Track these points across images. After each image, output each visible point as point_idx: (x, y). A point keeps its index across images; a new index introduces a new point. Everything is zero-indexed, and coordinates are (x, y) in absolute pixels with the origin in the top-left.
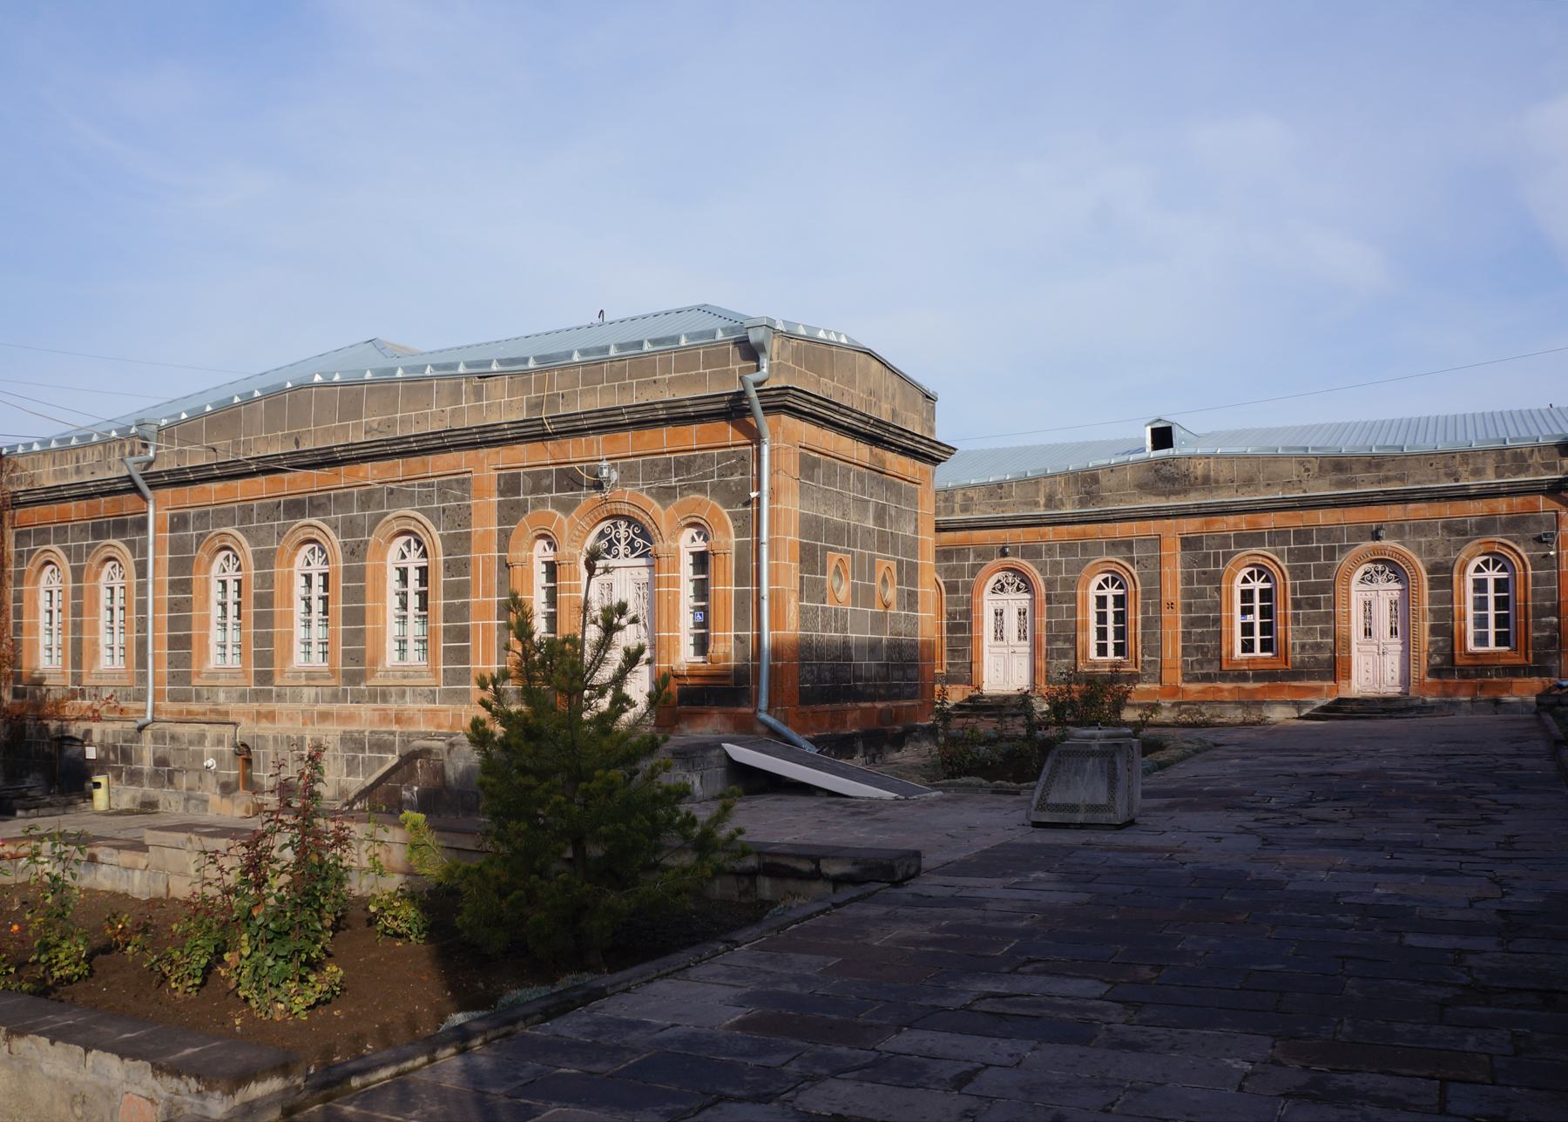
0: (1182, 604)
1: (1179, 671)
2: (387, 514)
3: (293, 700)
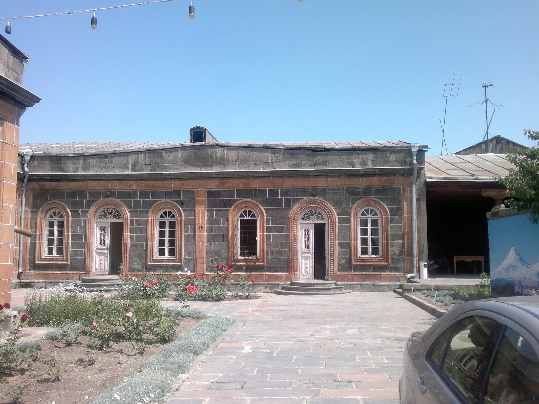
0: (207, 227)
1: (205, 264)
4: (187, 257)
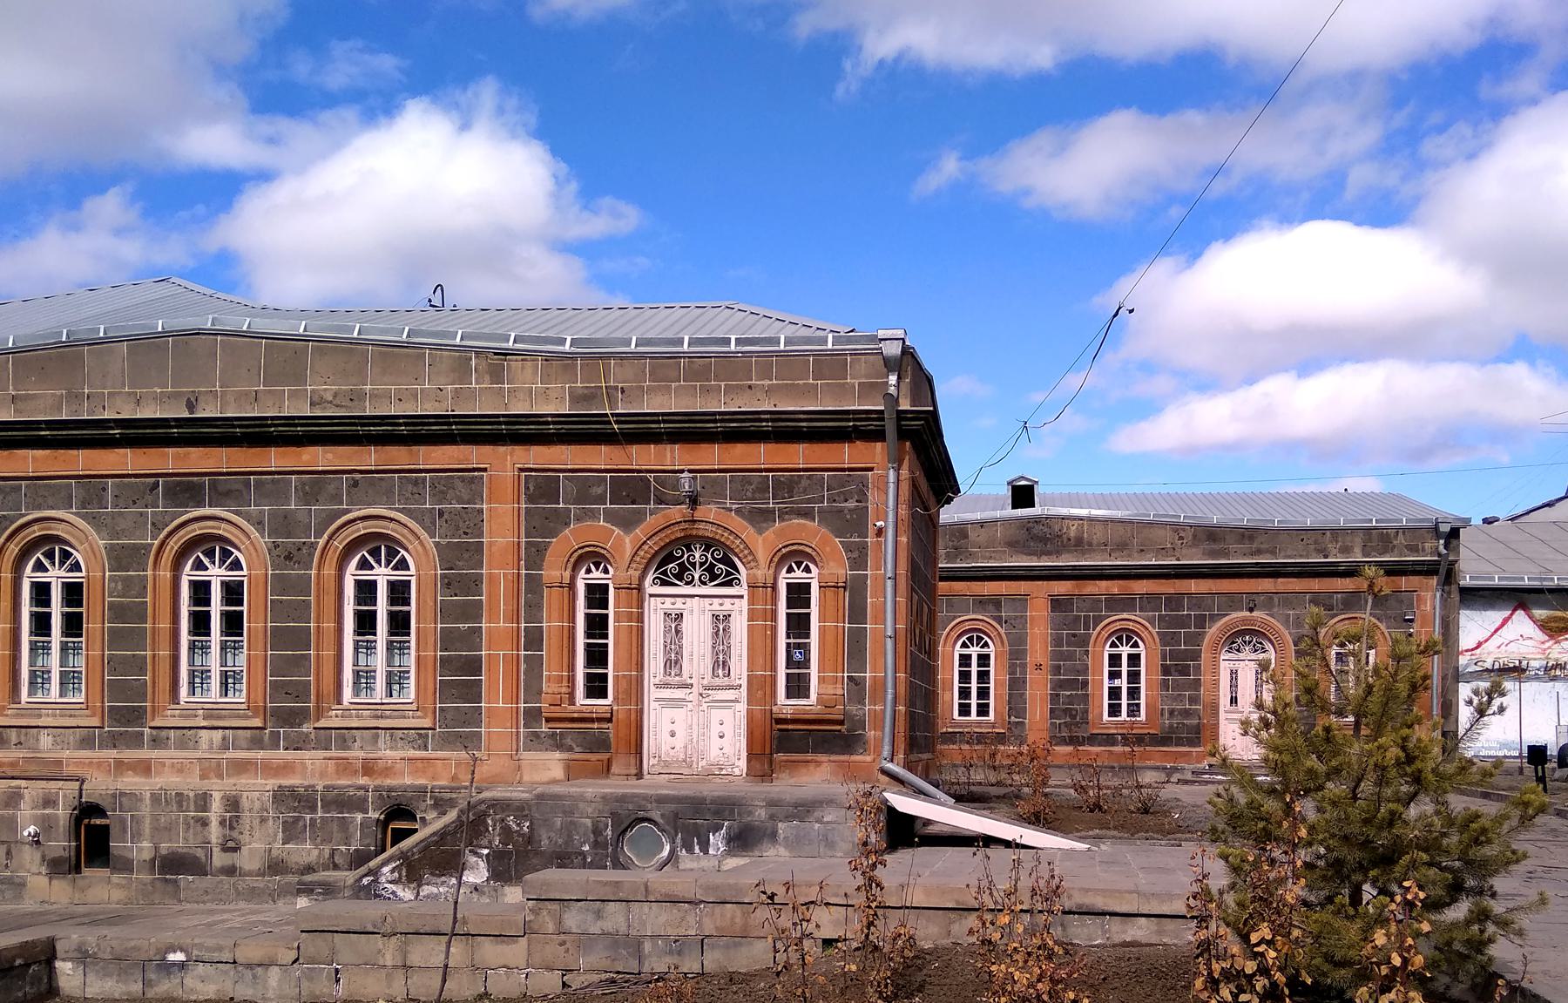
2: (348, 511)
3: (182, 745)
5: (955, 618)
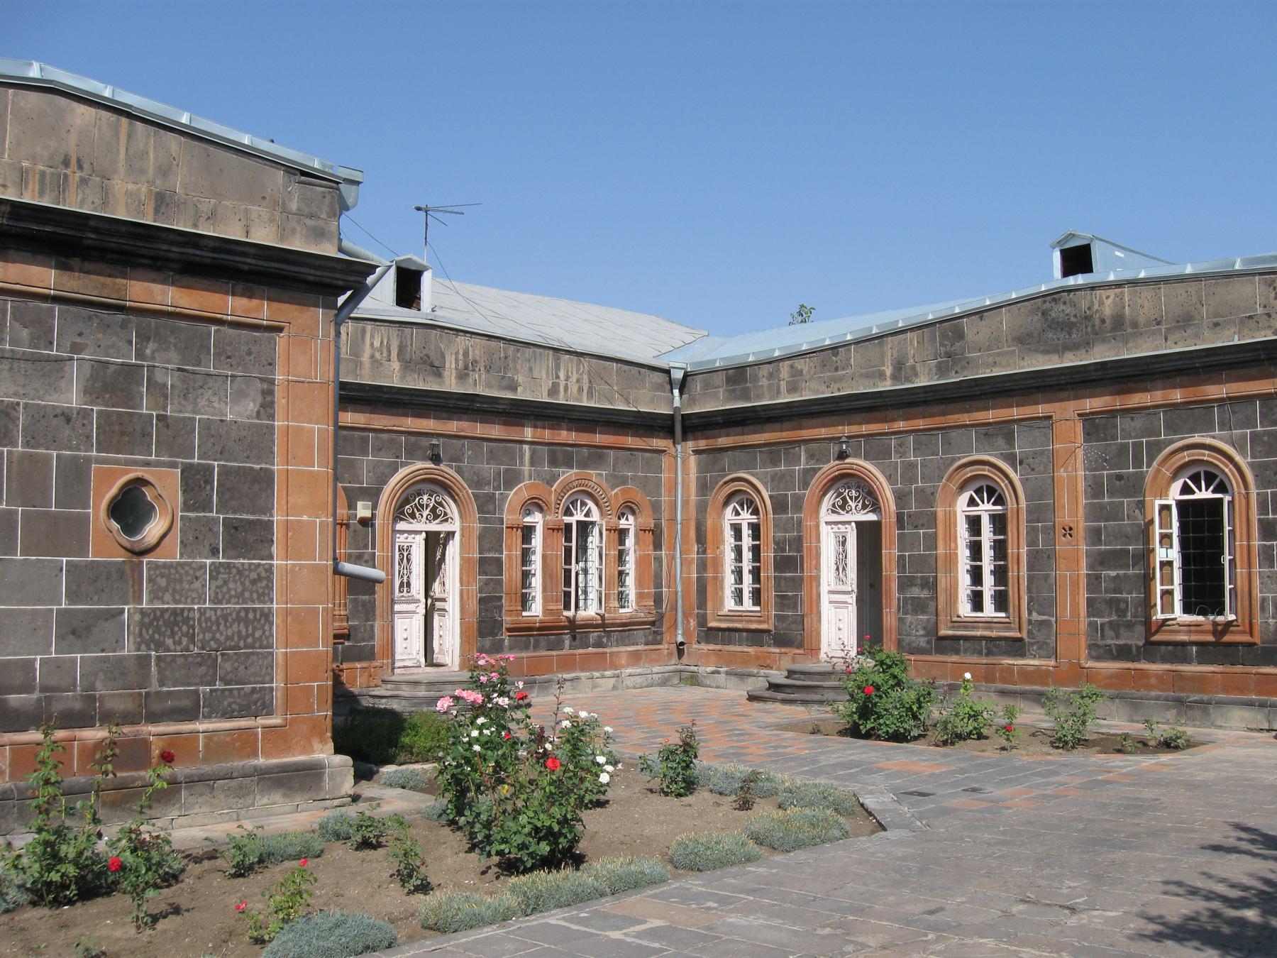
4: (1035, 616)
5: (953, 460)
